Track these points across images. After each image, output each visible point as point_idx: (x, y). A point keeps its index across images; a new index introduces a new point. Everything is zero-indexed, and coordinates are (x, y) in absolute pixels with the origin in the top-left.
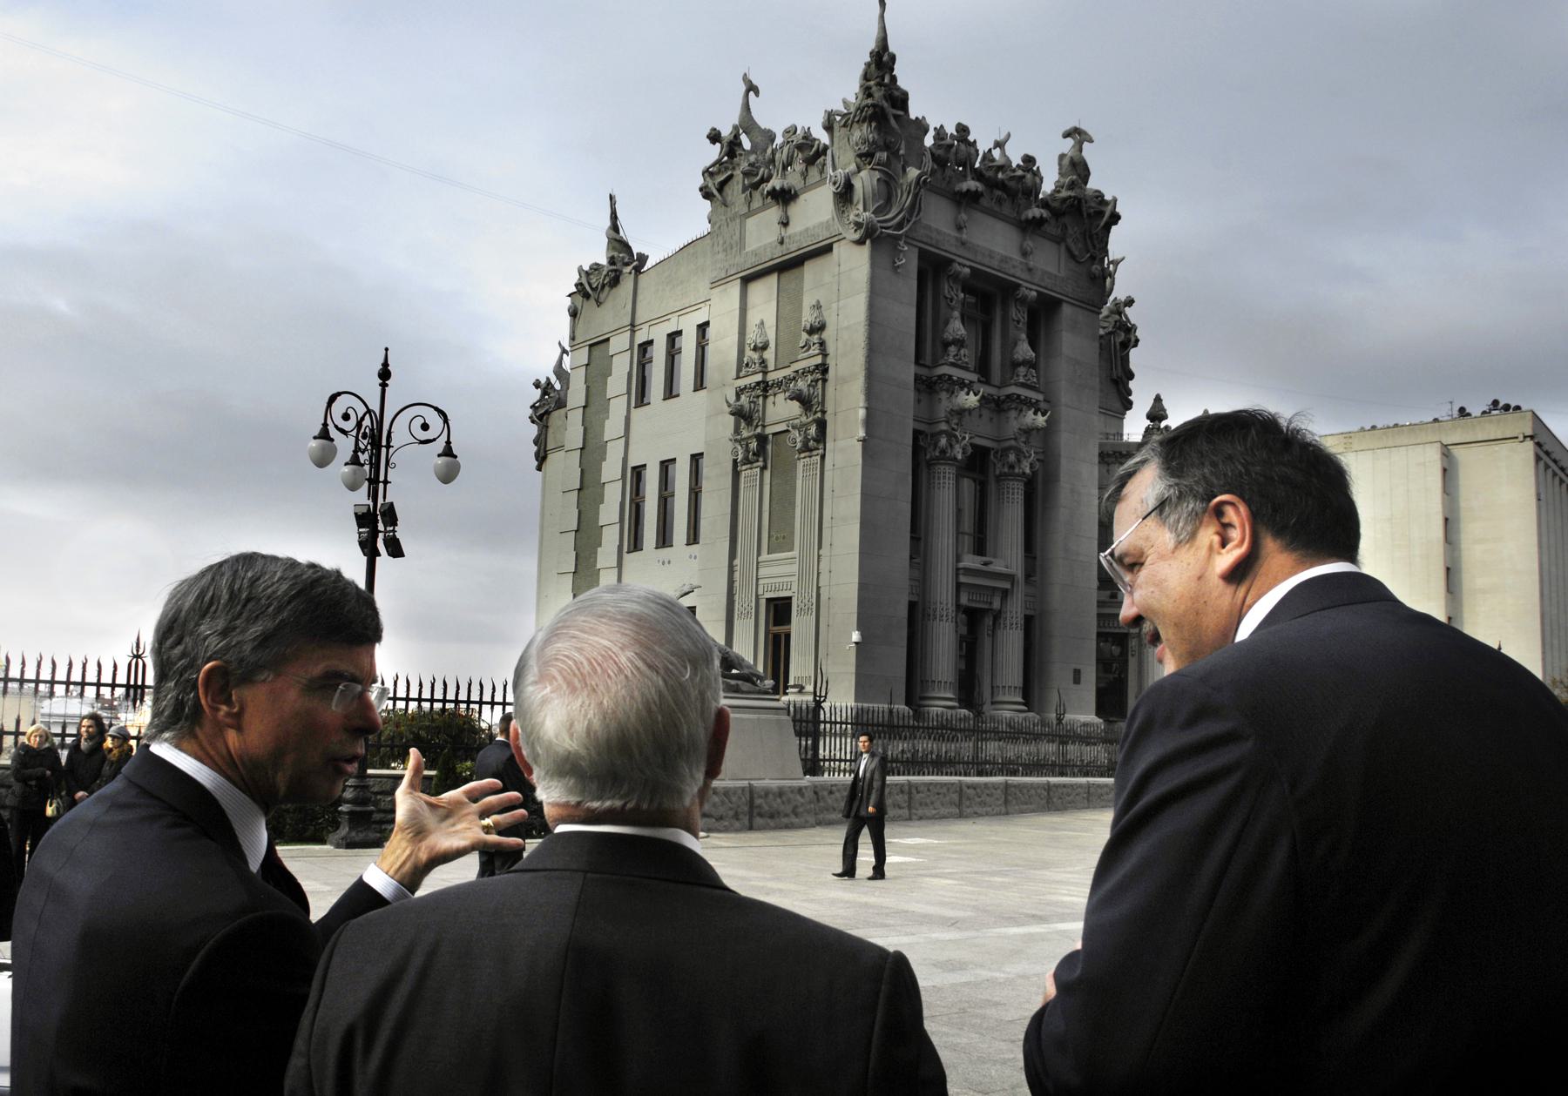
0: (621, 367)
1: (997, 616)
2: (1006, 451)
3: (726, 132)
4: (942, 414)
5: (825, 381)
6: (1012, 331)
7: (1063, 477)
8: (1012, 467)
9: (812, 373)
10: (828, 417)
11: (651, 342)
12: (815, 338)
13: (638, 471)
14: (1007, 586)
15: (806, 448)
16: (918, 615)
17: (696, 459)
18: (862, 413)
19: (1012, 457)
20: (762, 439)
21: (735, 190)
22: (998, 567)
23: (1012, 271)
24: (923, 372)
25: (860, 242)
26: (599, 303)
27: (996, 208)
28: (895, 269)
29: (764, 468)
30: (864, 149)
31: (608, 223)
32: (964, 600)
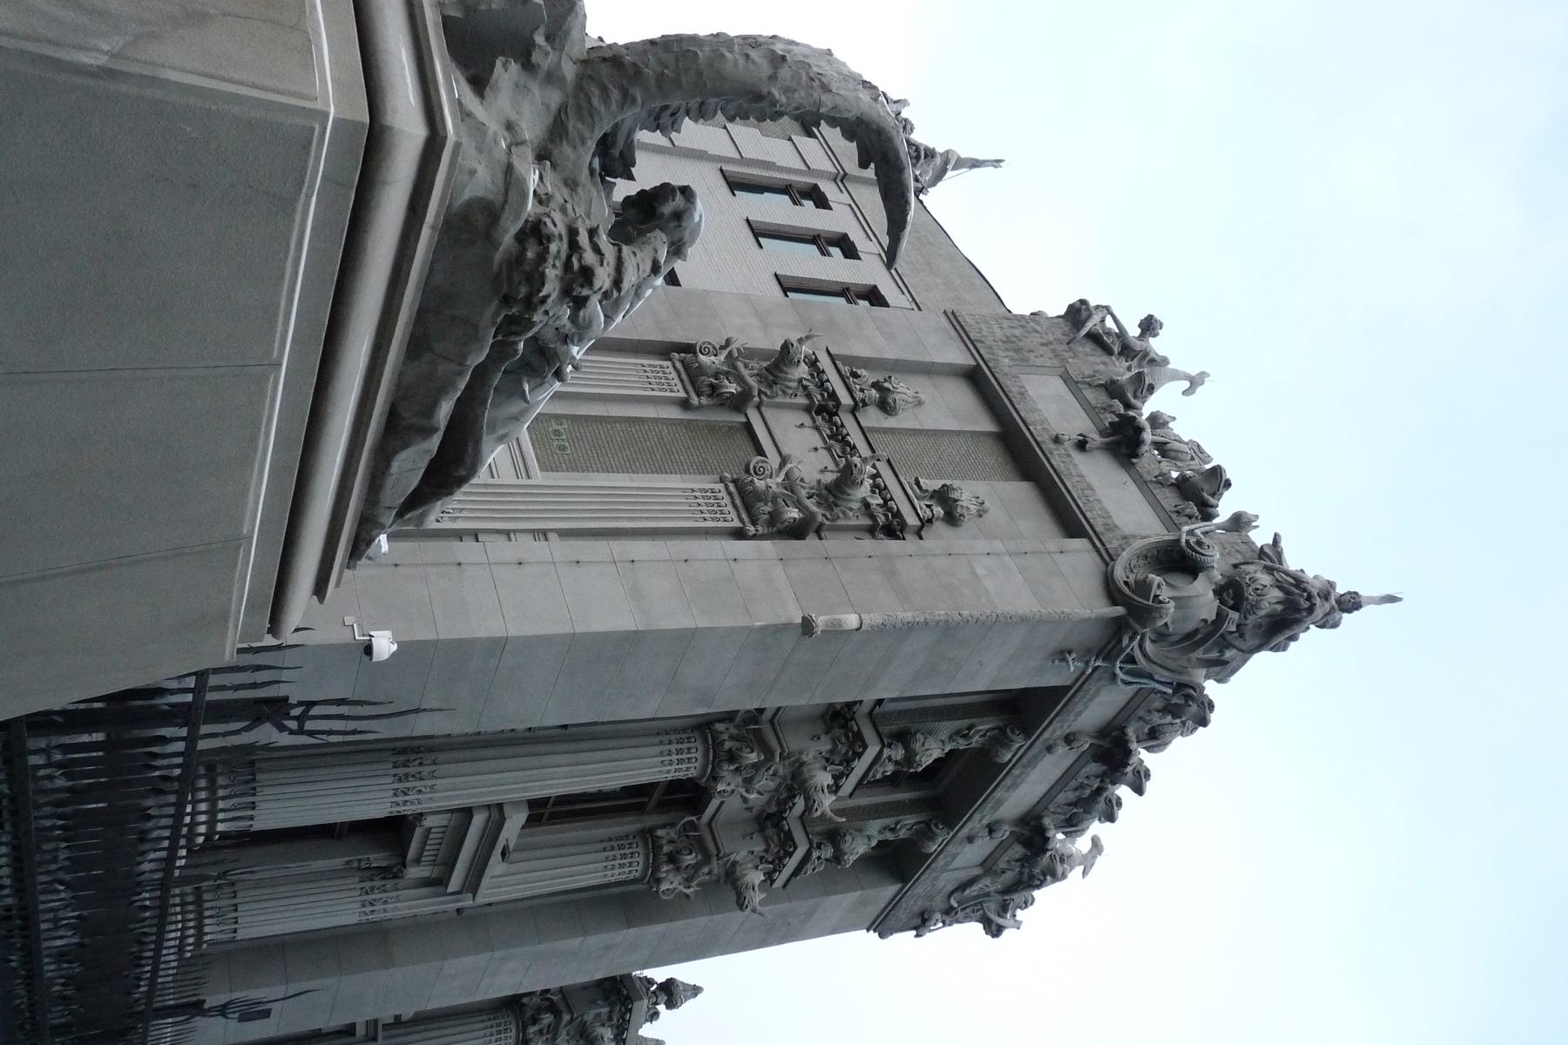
1: (391, 873)
3: (1157, 345)
4: (794, 742)
5: (871, 531)
10: (811, 541)
11: (822, 202)
12: (939, 510)
15: (747, 498)
18: (851, 621)
19: (690, 859)
20: (738, 403)
21: (1090, 362)
23: (977, 817)
24: (865, 708)
25: (1112, 592)
27: (1073, 784)
28: (1062, 654)
29: (685, 404)
30: (1250, 593)
31: (964, 154)
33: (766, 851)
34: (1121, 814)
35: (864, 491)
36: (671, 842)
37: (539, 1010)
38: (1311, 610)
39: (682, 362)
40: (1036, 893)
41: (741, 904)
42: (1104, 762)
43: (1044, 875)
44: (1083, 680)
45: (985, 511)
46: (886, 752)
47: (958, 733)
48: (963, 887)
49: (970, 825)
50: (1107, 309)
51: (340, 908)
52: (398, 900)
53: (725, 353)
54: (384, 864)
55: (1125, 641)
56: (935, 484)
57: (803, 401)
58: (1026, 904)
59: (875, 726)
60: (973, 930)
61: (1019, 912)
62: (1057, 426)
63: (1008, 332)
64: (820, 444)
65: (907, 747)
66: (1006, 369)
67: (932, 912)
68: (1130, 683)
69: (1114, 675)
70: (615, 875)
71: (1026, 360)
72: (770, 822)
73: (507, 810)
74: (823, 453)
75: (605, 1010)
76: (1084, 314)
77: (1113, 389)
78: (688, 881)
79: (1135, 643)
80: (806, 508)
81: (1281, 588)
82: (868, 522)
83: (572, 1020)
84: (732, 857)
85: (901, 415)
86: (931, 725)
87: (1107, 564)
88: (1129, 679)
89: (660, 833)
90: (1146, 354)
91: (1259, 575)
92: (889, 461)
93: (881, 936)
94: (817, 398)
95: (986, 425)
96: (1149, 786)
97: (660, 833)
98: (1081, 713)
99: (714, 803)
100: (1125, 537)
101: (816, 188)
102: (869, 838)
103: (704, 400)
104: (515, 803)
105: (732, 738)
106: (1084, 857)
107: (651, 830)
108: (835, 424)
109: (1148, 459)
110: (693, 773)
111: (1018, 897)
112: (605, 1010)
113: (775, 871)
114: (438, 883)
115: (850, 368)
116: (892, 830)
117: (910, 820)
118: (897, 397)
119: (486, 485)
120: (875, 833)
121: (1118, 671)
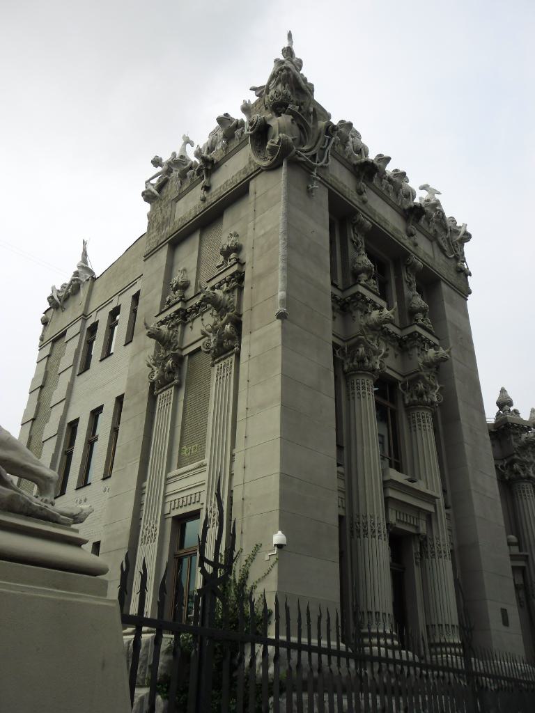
0: (72, 346)
1: (424, 541)
2: (414, 382)
3: (166, 158)
5: (241, 289)
6: (407, 293)
7: (462, 417)
8: (420, 395)
9: (228, 282)
10: (244, 319)
13: (73, 425)
14: (431, 509)
16: (349, 529)
17: (120, 400)
18: (281, 294)
19: (421, 386)
20: (179, 360)
21: (173, 189)
22: (420, 486)
23: (402, 240)
26: (64, 309)
28: (309, 192)
29: (178, 387)
31: (80, 259)
32: (393, 519)
33: (418, 347)
34: (402, 169)
35: (219, 293)
36: (412, 396)
37: (512, 470)
38: (288, 69)
39: (159, 389)
40: (447, 215)
41: (445, 360)
42: (373, 175)
43: (436, 210)
44: (324, 182)
45: (235, 233)
46: (362, 282)
47: (355, 248)
48: (443, 251)
49: (407, 245)
50: (148, 182)
51: (443, 571)
52: (438, 539)
53: (153, 367)
54: (418, 545)
55: (302, 159)
56: (222, 258)
57: (179, 329)
58: (453, 220)
59: (349, 288)
60: (467, 247)
61: (458, 225)
62: (197, 202)
63: (155, 229)
64: (200, 318)
65: (360, 272)
66: (171, 228)
67: (457, 267)
68: (328, 159)
69: (322, 166)
70: (429, 426)
71: (167, 219)
72: (404, 346)
73: (387, 478)
74: (205, 316)
75: (513, 437)
76: (149, 193)
77: (183, 176)
78: (434, 388)
79: (303, 154)
80: (226, 320)
81: (277, 84)
82: (236, 291)
83: (518, 454)
84: (420, 364)
85: (189, 279)
86: (350, 261)
87: (262, 171)
88: (325, 159)
89: (407, 402)
90: (169, 163)
91: (270, 95)
92: (208, 282)
93: (470, 293)
94: (178, 320)
95: (196, 237)
96: (386, 154)
97: (407, 402)
98: (345, 186)
99: (388, 371)
100: (250, 163)
101: (89, 329)
102: (414, 295)
103: (176, 377)
104: (384, 472)
105: (352, 361)
106: (430, 193)
107: (406, 406)
108: (191, 311)
109: (216, 156)
110: (371, 382)
111: (449, 224)
112: (513, 437)
113: (429, 343)
114: (429, 517)
115: (166, 304)
116: (410, 284)
117: (405, 275)
118: (180, 280)
119: (209, 487)
120: (412, 293)
121: (320, 164)
